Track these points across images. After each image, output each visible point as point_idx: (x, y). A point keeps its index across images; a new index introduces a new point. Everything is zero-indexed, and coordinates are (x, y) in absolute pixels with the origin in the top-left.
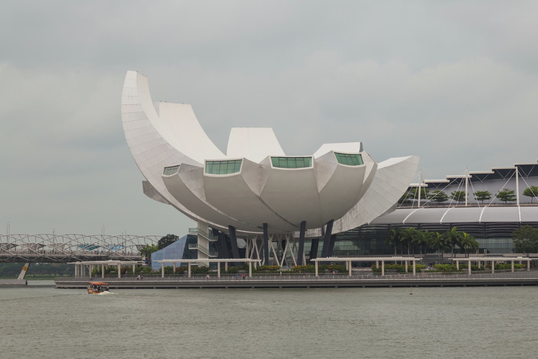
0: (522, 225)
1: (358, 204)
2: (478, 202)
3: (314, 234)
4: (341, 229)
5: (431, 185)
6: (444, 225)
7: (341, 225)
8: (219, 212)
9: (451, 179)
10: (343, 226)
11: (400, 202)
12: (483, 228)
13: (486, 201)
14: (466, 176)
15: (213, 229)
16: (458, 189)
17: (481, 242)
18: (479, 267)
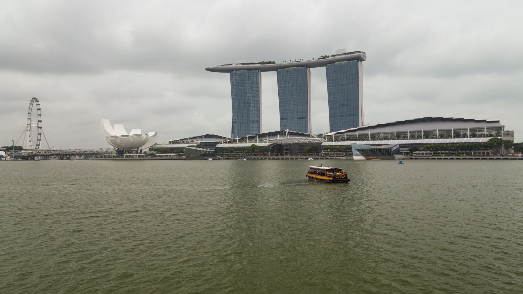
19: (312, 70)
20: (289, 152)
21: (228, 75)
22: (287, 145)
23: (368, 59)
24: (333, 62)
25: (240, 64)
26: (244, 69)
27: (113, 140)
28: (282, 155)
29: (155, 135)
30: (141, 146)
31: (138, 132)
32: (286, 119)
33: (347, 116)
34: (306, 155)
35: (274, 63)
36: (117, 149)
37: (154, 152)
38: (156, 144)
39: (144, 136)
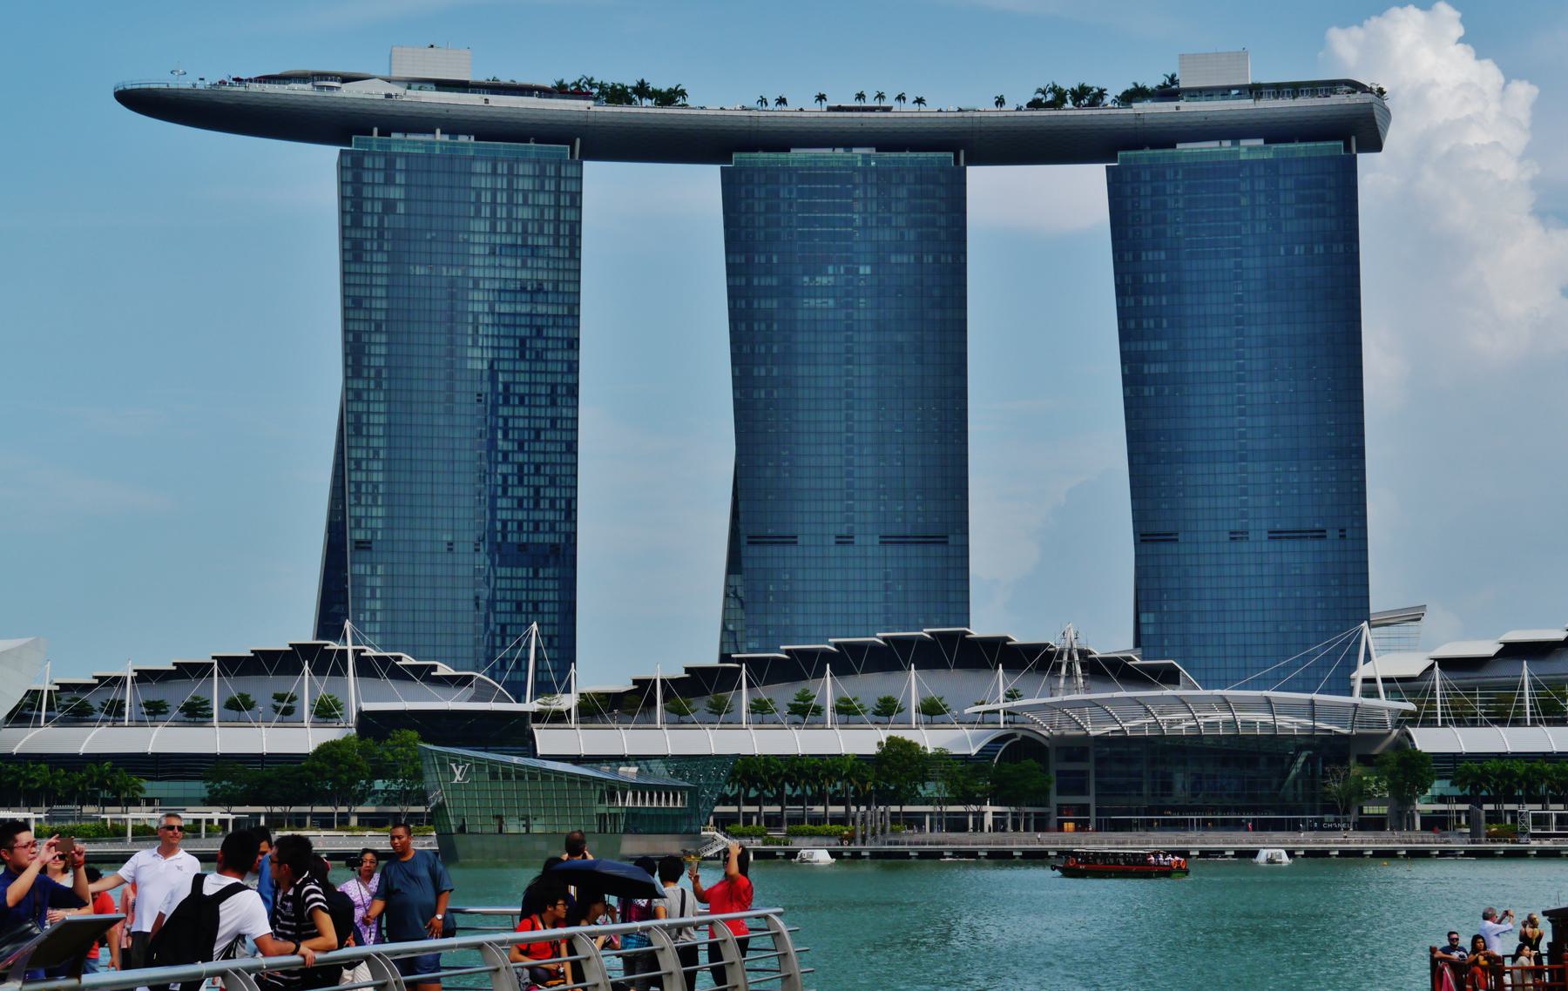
5: (65, 687)
6: (86, 756)
9: (101, 679)
11: (9, 716)
14: (130, 674)
16: (114, 694)
17: (151, 788)
19: (977, 176)
20: (1090, 800)
21: (320, 163)
22: (1077, 748)
23: (1387, 143)
24: (1164, 137)
25: (423, 82)
26: (454, 125)
28: (1041, 825)
32: (791, 540)
33: (1275, 535)
34: (1238, 825)
35: (668, 98)
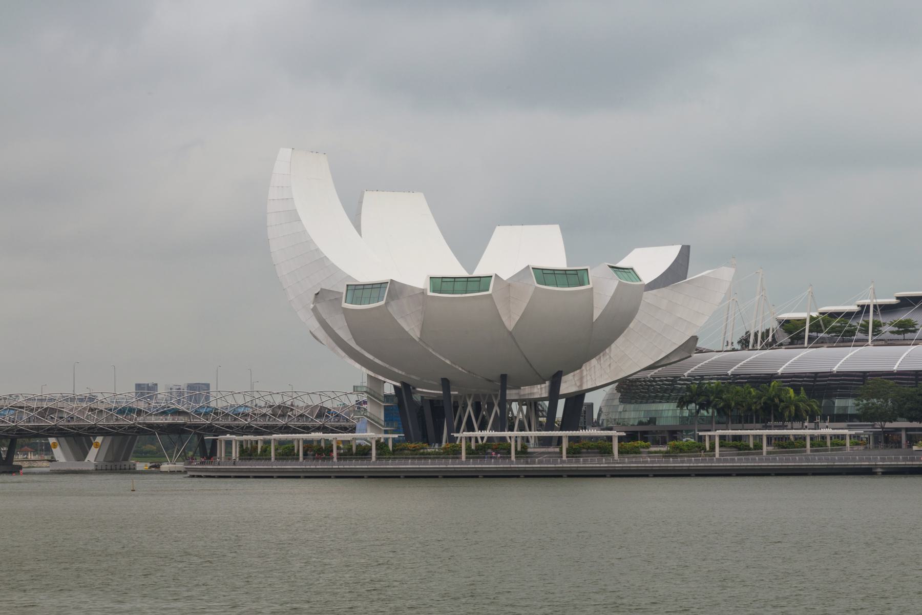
0: (871, 376)
1: (613, 346)
2: (896, 336)
3: (533, 393)
4: (581, 385)
7: (581, 379)
8: (377, 361)
10: (585, 380)
12: (912, 379)
13: (908, 335)
15: (403, 383)
18: (751, 446)
27: (363, 317)
29: (676, 273)
30: (576, 364)
31: (547, 248)
36: (389, 388)
37: (668, 412)
38: (691, 346)
39: (603, 288)
